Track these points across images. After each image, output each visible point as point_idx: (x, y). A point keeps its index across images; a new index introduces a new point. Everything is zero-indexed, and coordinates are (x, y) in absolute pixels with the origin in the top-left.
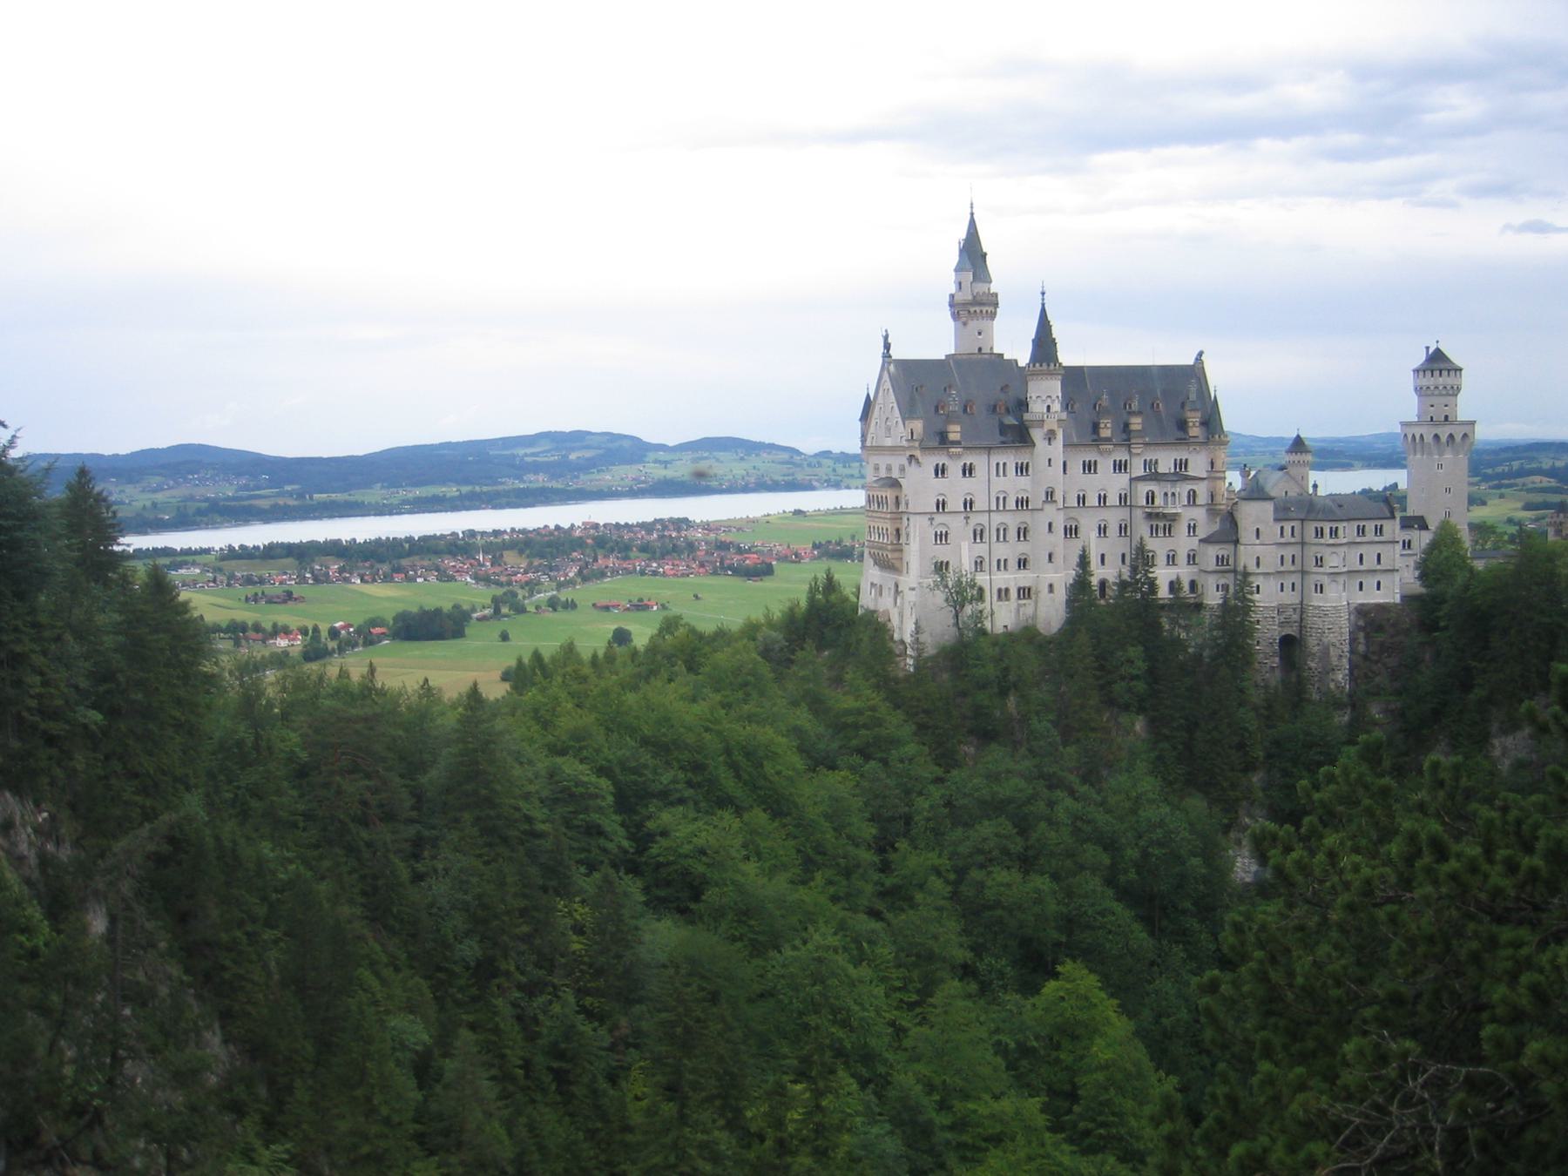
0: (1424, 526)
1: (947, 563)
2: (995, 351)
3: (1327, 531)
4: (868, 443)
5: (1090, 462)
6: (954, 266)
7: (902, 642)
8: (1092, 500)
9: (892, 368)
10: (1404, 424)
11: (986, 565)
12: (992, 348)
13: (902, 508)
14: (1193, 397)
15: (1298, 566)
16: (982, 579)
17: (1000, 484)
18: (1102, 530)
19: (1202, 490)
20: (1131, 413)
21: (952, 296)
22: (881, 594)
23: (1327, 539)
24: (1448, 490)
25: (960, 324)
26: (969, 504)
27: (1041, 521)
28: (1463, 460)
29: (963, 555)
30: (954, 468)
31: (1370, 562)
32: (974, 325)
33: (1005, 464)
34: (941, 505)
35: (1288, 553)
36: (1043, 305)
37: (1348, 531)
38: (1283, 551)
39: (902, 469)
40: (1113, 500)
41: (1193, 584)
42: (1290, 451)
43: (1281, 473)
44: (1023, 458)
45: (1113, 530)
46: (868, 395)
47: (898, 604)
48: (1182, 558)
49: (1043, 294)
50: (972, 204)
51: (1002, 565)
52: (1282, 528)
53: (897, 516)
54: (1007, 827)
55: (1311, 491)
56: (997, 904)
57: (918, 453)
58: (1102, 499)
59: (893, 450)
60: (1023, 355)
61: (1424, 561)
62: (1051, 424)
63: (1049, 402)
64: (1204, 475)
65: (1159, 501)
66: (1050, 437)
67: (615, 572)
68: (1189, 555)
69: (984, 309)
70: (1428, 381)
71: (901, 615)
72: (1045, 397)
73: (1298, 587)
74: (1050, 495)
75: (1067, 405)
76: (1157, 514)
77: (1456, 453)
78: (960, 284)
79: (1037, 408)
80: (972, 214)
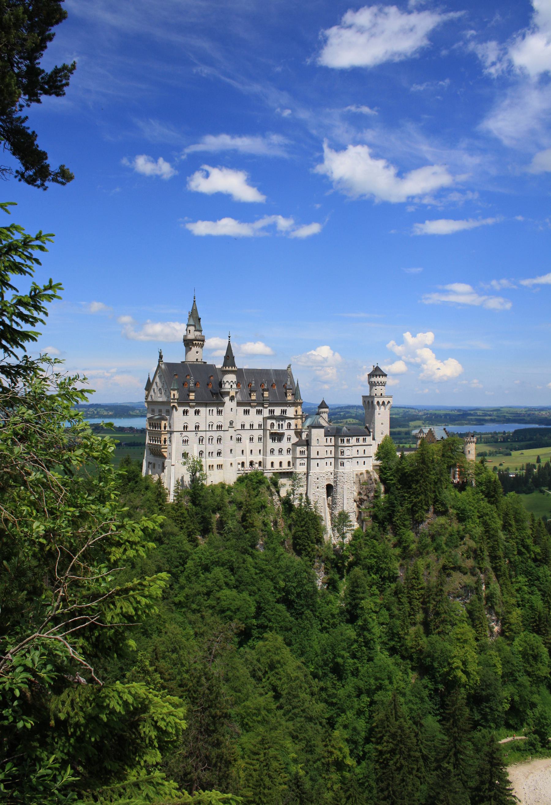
4: (149, 399)
8: (247, 427)
10: (364, 397)
11: (204, 455)
14: (289, 383)
15: (333, 455)
17: (210, 418)
18: (251, 439)
20: (264, 390)
22: (154, 467)
23: (346, 444)
24: (382, 424)
26: (197, 427)
27: (228, 434)
28: (387, 412)
29: (194, 450)
30: (191, 411)
32: (194, 349)
34: (185, 427)
35: (329, 449)
37: (353, 440)
40: (256, 426)
41: (289, 462)
43: (318, 416)
44: (220, 408)
45: (256, 439)
51: (211, 454)
54: (228, 572)
58: (251, 426)
61: (379, 453)
64: (293, 417)
65: (276, 427)
66: (232, 399)
70: (374, 379)
74: (231, 423)
79: (226, 387)
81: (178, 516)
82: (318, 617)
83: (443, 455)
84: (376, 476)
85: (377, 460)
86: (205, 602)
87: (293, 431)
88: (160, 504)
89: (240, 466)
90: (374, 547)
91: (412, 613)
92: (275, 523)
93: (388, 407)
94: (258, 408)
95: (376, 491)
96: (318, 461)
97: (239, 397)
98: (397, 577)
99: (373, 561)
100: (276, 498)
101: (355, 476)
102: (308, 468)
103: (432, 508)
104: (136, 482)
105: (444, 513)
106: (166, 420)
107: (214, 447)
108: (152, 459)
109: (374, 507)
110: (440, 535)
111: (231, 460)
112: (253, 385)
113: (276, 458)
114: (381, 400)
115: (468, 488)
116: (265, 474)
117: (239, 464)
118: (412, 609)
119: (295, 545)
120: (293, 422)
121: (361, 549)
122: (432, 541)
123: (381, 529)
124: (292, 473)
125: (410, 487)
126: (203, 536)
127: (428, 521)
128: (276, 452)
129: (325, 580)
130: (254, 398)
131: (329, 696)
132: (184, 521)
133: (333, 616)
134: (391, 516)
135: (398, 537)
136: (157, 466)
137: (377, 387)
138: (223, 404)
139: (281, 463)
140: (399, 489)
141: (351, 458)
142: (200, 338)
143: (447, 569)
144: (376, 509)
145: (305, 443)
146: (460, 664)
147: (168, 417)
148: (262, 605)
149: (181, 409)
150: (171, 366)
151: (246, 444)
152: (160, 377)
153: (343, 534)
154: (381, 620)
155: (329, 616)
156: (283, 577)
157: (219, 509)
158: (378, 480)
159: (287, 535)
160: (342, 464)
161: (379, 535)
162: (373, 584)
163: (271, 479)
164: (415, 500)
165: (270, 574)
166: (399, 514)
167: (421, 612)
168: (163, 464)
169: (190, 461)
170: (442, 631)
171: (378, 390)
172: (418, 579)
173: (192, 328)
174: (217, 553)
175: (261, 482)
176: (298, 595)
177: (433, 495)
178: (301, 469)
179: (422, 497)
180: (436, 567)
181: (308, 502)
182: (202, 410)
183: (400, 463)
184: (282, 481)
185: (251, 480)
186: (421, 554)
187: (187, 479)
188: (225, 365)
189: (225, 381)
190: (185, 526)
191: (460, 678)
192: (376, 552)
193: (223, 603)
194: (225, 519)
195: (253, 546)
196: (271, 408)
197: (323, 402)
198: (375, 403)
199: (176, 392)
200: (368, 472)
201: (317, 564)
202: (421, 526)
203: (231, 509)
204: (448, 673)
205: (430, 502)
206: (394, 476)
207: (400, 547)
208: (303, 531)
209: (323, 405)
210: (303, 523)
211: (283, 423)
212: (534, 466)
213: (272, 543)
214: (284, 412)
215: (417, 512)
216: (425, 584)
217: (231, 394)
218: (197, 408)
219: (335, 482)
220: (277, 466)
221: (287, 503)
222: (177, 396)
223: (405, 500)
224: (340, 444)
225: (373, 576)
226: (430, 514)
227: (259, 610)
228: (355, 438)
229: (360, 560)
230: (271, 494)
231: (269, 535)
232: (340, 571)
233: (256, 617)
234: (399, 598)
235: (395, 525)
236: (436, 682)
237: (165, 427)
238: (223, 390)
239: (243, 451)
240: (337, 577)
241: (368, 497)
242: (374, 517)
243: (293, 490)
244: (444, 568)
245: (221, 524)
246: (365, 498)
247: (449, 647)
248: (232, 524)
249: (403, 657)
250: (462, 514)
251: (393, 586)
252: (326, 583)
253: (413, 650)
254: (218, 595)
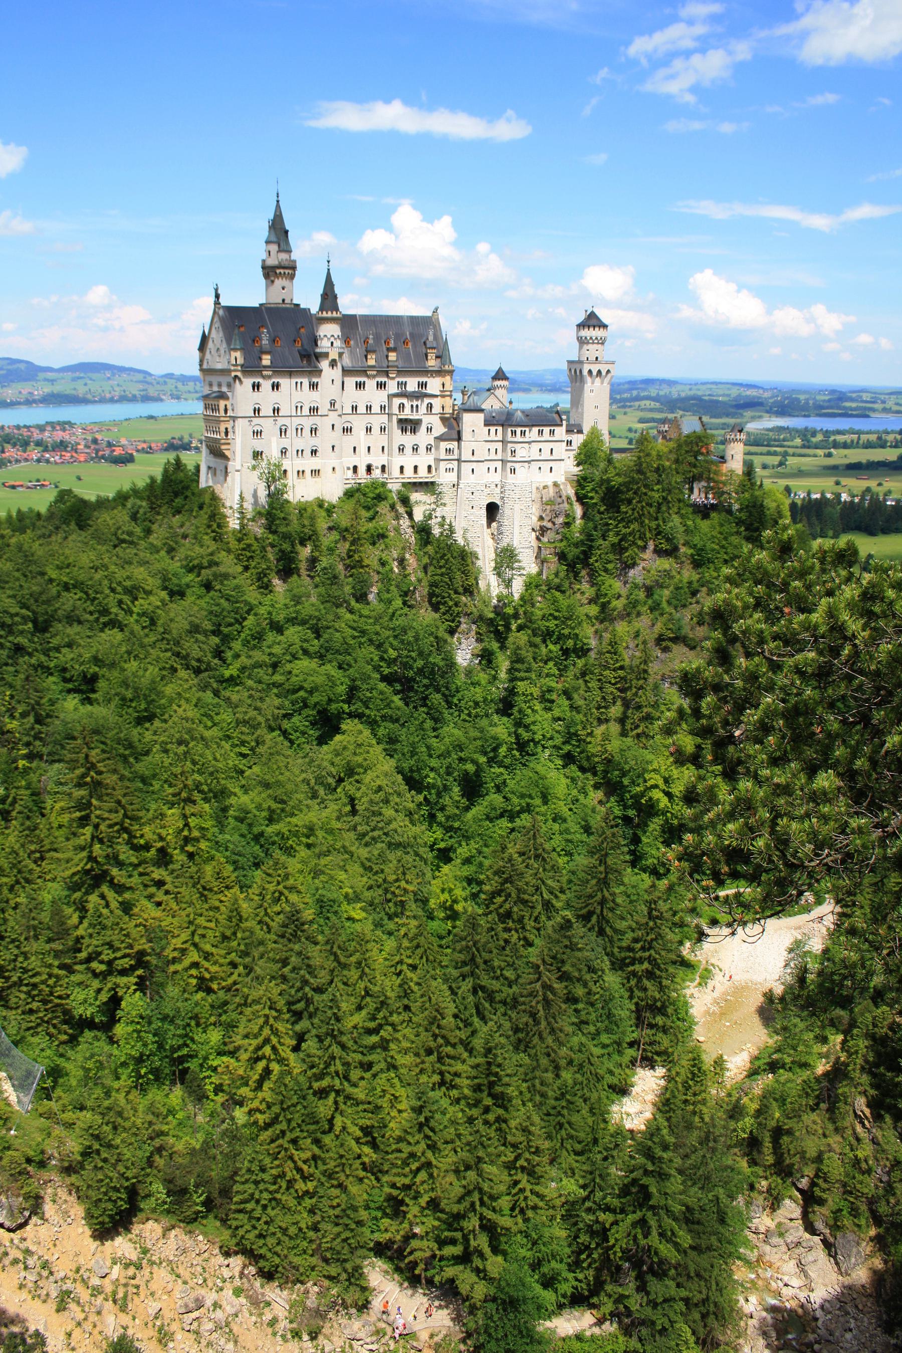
0: (580, 432)
2: (295, 302)
3: (518, 433)
4: (205, 366)
6: (265, 239)
7: (231, 508)
8: (362, 409)
9: (221, 312)
10: (570, 362)
13: (230, 413)
14: (431, 338)
15: (499, 456)
16: (286, 464)
18: (369, 430)
19: (437, 403)
21: (264, 261)
23: (519, 438)
24: (596, 407)
26: (276, 410)
28: (606, 387)
29: (272, 447)
30: (266, 385)
31: (546, 455)
32: (279, 282)
34: (257, 411)
35: (493, 446)
38: (489, 445)
40: (376, 409)
41: (429, 467)
42: (495, 378)
44: (315, 380)
45: (376, 430)
48: (422, 449)
51: (300, 452)
55: (507, 405)
56: (301, 688)
58: (369, 408)
60: (314, 308)
62: (334, 355)
63: (332, 339)
64: (438, 393)
65: (407, 410)
66: (333, 364)
67: (18, 461)
69: (287, 271)
70: (586, 333)
72: (329, 335)
74: (333, 404)
75: (346, 341)
76: (406, 420)
77: (602, 383)
79: (324, 345)
81: (244, 549)
82: (456, 705)
83: (677, 461)
84: (570, 491)
85: (578, 465)
86: (266, 677)
87: (437, 417)
88: (213, 531)
89: (350, 473)
90: (555, 601)
91: (603, 706)
92: (402, 561)
93: (607, 380)
94: (380, 379)
95: (567, 516)
96: (474, 465)
97: (347, 361)
98: (589, 650)
99: (552, 624)
100: (405, 523)
101: (534, 490)
102: (459, 477)
103: (651, 545)
104: (186, 497)
105: (671, 552)
106: (227, 398)
107: (306, 442)
108: (214, 462)
109: (562, 540)
110: (661, 587)
111: (334, 462)
112: (371, 341)
113: (409, 460)
114: (595, 369)
115: (713, 515)
116: (390, 486)
117: (348, 469)
118: (604, 698)
119: (431, 595)
120: (437, 403)
121: (533, 605)
122: (647, 597)
123: (571, 575)
124: (433, 483)
125: (618, 512)
126: (285, 581)
127: (642, 564)
128: (408, 450)
129: (477, 652)
130: (372, 362)
131: (448, 818)
132: (252, 557)
133: (477, 704)
134: (587, 555)
135: (595, 588)
136: (218, 472)
137: (590, 347)
138: (319, 372)
139: (416, 467)
140: (602, 513)
141: (529, 462)
142: (286, 264)
143: (664, 640)
144: (564, 543)
145: (456, 437)
146: (661, 782)
147: (229, 394)
148: (358, 683)
149: (248, 382)
150: (234, 312)
151: (360, 437)
152: (217, 329)
153: (510, 581)
154: (557, 713)
155: (471, 704)
156: (395, 643)
157: (310, 538)
158: (574, 499)
159: (419, 581)
160: (513, 471)
161: (566, 585)
162: (550, 659)
163: (399, 492)
164: (624, 531)
165: (375, 638)
166: (599, 552)
167: (619, 703)
168: (226, 468)
169: (264, 464)
170: (644, 733)
171: (592, 351)
172: (615, 654)
173: (274, 248)
174: (295, 605)
175: (380, 498)
176: (420, 671)
177: (653, 524)
178: (445, 478)
179: (634, 526)
180: (650, 635)
181: (452, 530)
182: (285, 382)
183: (606, 471)
184: (415, 497)
185: (364, 495)
186: (628, 615)
187: (263, 494)
188: (322, 309)
189: (322, 334)
190: (253, 564)
191: (658, 800)
192: (557, 611)
193: (294, 679)
194: (317, 554)
195: (362, 597)
196: (400, 380)
197: (500, 370)
198: (585, 372)
199: (238, 354)
200: (556, 484)
201: (463, 626)
202: (632, 573)
203: (328, 539)
204: (643, 794)
205: (648, 535)
206: (597, 492)
207: (596, 603)
208: (442, 575)
209: (500, 375)
210: (442, 562)
211: (419, 403)
213: (388, 591)
214: (423, 385)
215: (626, 549)
216: (627, 662)
217: (331, 357)
218: (276, 381)
219: (502, 498)
221: (423, 531)
222: (240, 361)
223: (609, 530)
224: (510, 439)
225: (551, 647)
226: (648, 554)
227: (353, 691)
228: (535, 430)
229: (530, 621)
230: (398, 517)
231: (386, 579)
232: (501, 638)
233: (348, 701)
234: (586, 682)
235: (592, 570)
236: (625, 807)
237: (226, 411)
238: (318, 350)
240: (495, 646)
241: (554, 524)
242: (562, 556)
243: (434, 510)
244: (660, 640)
245: (313, 561)
246: (549, 525)
247: (650, 757)
248: (324, 562)
249: (583, 770)
250: (699, 555)
251: (580, 663)
252: (478, 656)
253: (596, 759)
254: (288, 667)
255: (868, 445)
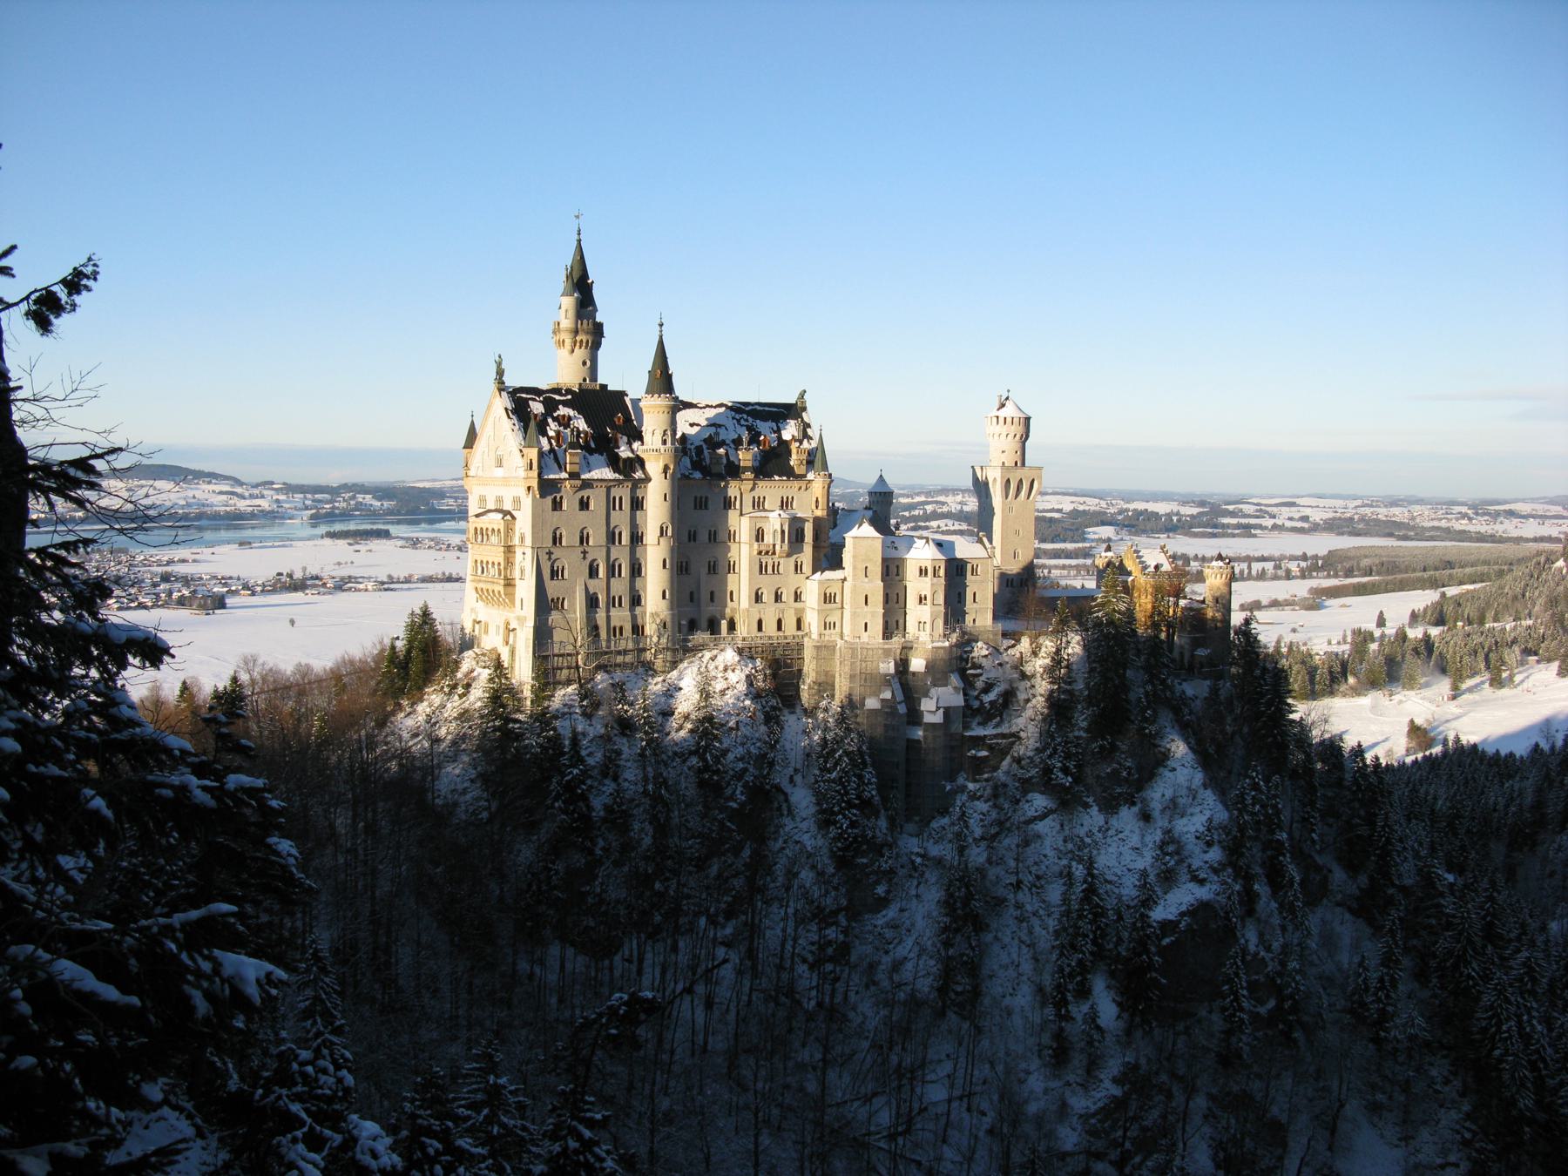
1: (564, 599)
2: (601, 380)
5: (701, 498)
12: (596, 381)
22: (486, 632)
24: (1017, 532)
25: (564, 353)
26: (583, 539)
33: (621, 499)
34: (556, 540)
36: (661, 337)
39: (517, 501)
45: (722, 568)
46: (472, 422)
47: (511, 642)
49: (661, 325)
50: (579, 231)
52: (887, 567)
53: (509, 550)
57: (535, 484)
59: (506, 481)
65: (768, 539)
68: (796, 593)
71: (513, 653)
73: (901, 622)
78: (566, 311)
80: (579, 241)
128: (768, 597)
136: (492, 629)
212: (1367, 637)
220: (770, 628)
239: (692, 593)
255: (1262, 576)
